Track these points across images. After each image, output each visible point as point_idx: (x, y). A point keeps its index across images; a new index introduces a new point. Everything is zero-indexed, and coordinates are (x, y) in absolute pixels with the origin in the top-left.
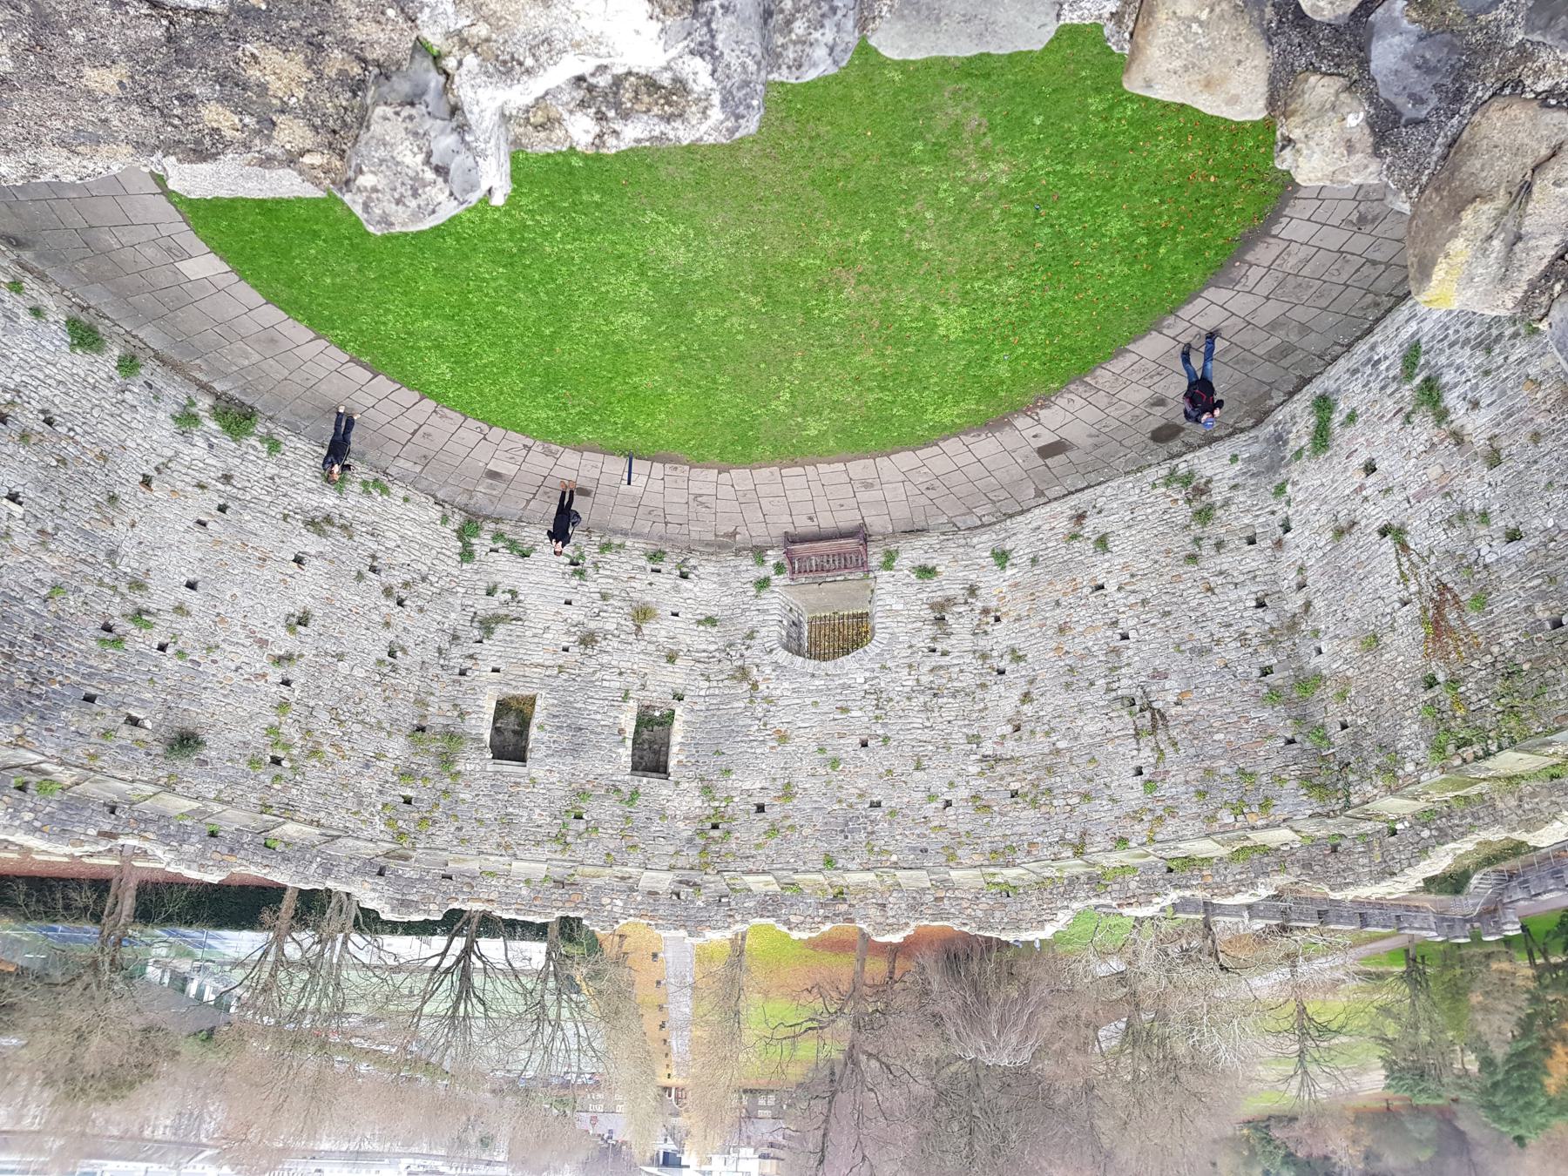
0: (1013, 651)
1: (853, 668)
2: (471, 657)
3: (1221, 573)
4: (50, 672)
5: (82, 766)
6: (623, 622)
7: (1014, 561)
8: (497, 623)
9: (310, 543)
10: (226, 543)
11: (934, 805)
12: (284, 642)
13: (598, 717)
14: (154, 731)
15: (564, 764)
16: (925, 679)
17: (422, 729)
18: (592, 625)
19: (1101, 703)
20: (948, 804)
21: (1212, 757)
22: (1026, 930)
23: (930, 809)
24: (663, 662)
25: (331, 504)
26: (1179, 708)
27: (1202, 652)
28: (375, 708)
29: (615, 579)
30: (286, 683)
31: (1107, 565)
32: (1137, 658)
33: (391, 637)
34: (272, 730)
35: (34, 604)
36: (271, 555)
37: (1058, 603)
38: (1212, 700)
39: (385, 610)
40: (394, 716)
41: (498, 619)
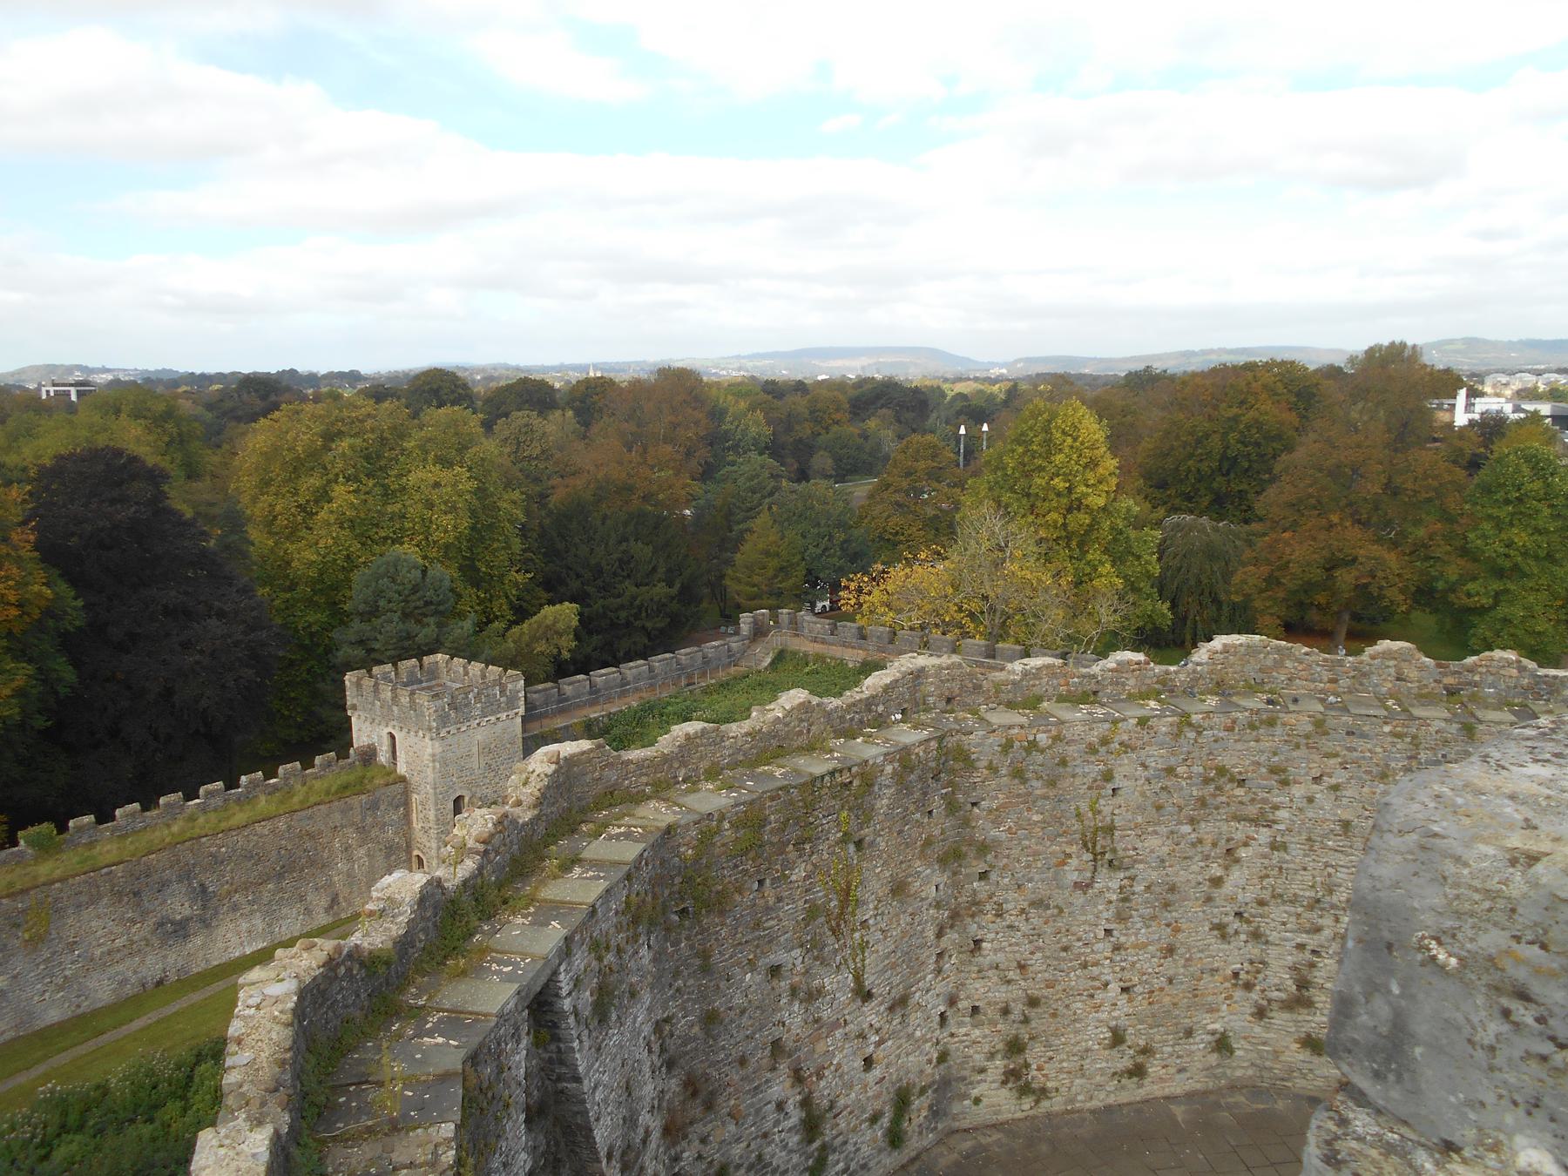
3: (1009, 982)
7: (1209, 1038)
11: (1333, 781)
16: (1327, 921)
19: (1141, 866)
20: (1317, 780)
21: (1046, 797)
22: (1241, 645)
23: (1340, 777)
26: (1068, 851)
27: (1039, 904)
31: (1115, 1014)
32: (1100, 907)
37: (1170, 981)
38: (1036, 854)
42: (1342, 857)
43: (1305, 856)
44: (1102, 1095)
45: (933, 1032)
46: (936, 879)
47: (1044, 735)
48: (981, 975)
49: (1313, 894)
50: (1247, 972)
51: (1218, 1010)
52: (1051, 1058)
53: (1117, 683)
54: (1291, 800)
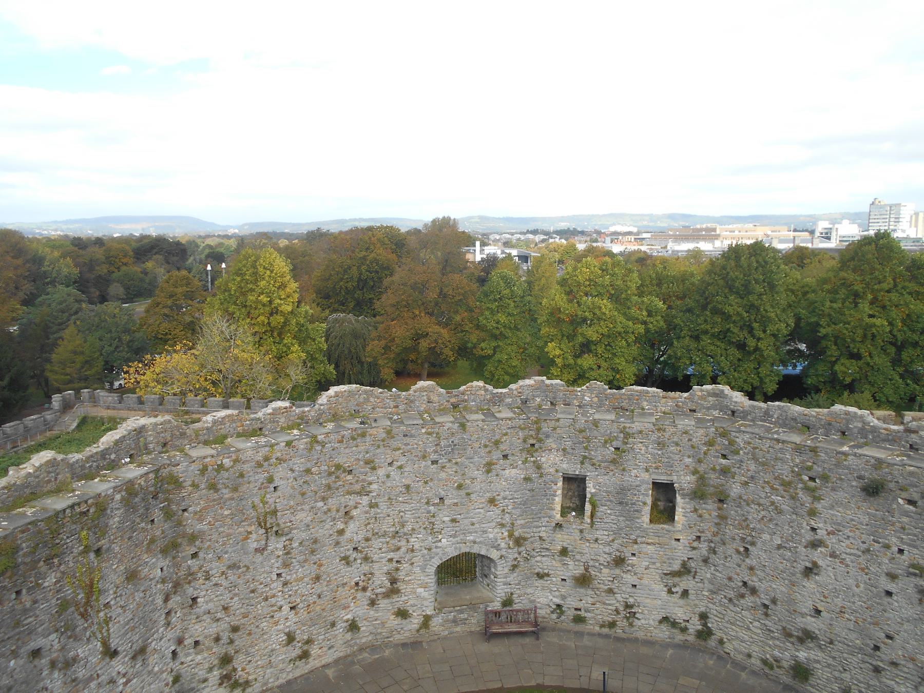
0: (348, 563)
1: (448, 548)
2: (694, 548)
3: (218, 620)
6: (598, 574)
7: (345, 624)
8: (680, 571)
9: (812, 624)
10: (870, 624)
11: (399, 464)
13: (609, 512)
15: (628, 481)
16: (403, 543)
17: (721, 501)
18: (617, 571)
20: (390, 464)
21: (233, 499)
22: (345, 391)
24: (570, 548)
25: (801, 653)
26: (249, 530)
27: (233, 566)
28: (754, 513)
29: (604, 604)
32: (272, 561)
33: (748, 560)
34: (817, 499)
36: (837, 615)
37: (319, 596)
38: (228, 535)
40: (738, 509)
42: (407, 505)
43: (388, 508)
44: (284, 675)
45: (168, 665)
46: (160, 564)
47: (228, 460)
48: (198, 620)
49: (394, 529)
50: (363, 581)
51: (349, 607)
52: (250, 661)
53: (274, 422)
54: (378, 478)
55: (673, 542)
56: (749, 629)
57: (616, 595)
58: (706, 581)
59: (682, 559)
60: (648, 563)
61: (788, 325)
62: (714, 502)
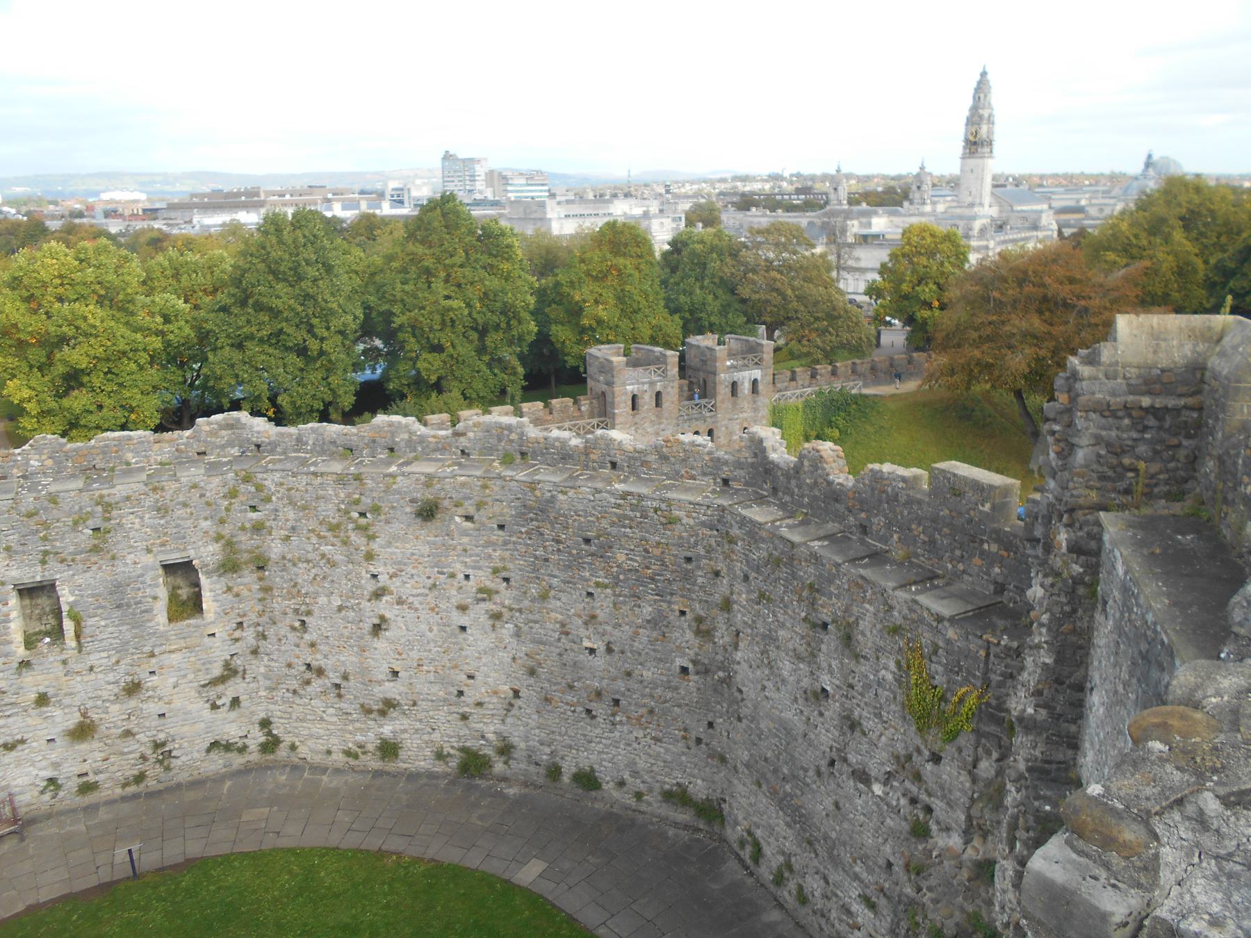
2: (237, 640)
4: (530, 539)
5: (490, 479)
8: (222, 676)
9: (392, 690)
10: (449, 669)
12: (385, 607)
13: (103, 623)
14: (452, 518)
15: (124, 572)
17: (261, 568)
18: (133, 703)
25: (386, 727)
28: (303, 574)
29: (123, 754)
30: (374, 576)
33: (307, 637)
34: (372, 538)
35: (555, 581)
39: (319, 656)
40: (284, 573)
41: (222, 680)
55: (207, 640)
56: (322, 719)
57: (137, 737)
58: (259, 678)
59: (223, 658)
60: (176, 679)
61: (356, 318)
62: (252, 572)
